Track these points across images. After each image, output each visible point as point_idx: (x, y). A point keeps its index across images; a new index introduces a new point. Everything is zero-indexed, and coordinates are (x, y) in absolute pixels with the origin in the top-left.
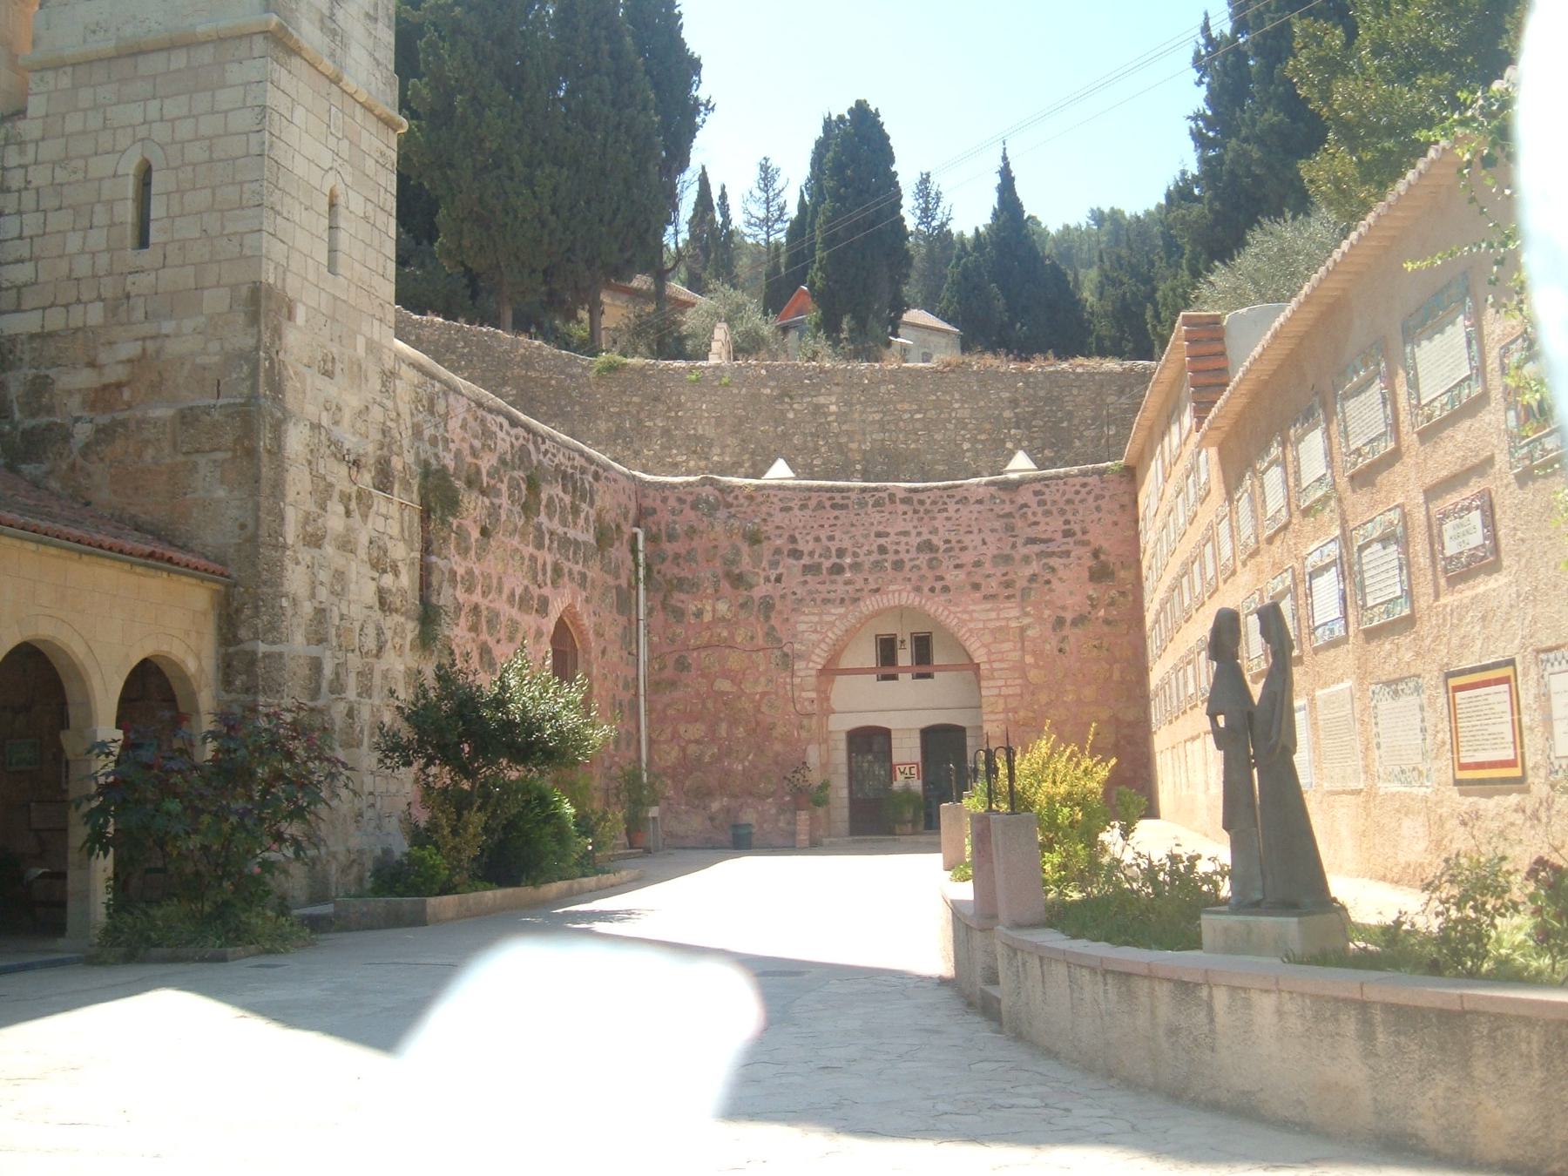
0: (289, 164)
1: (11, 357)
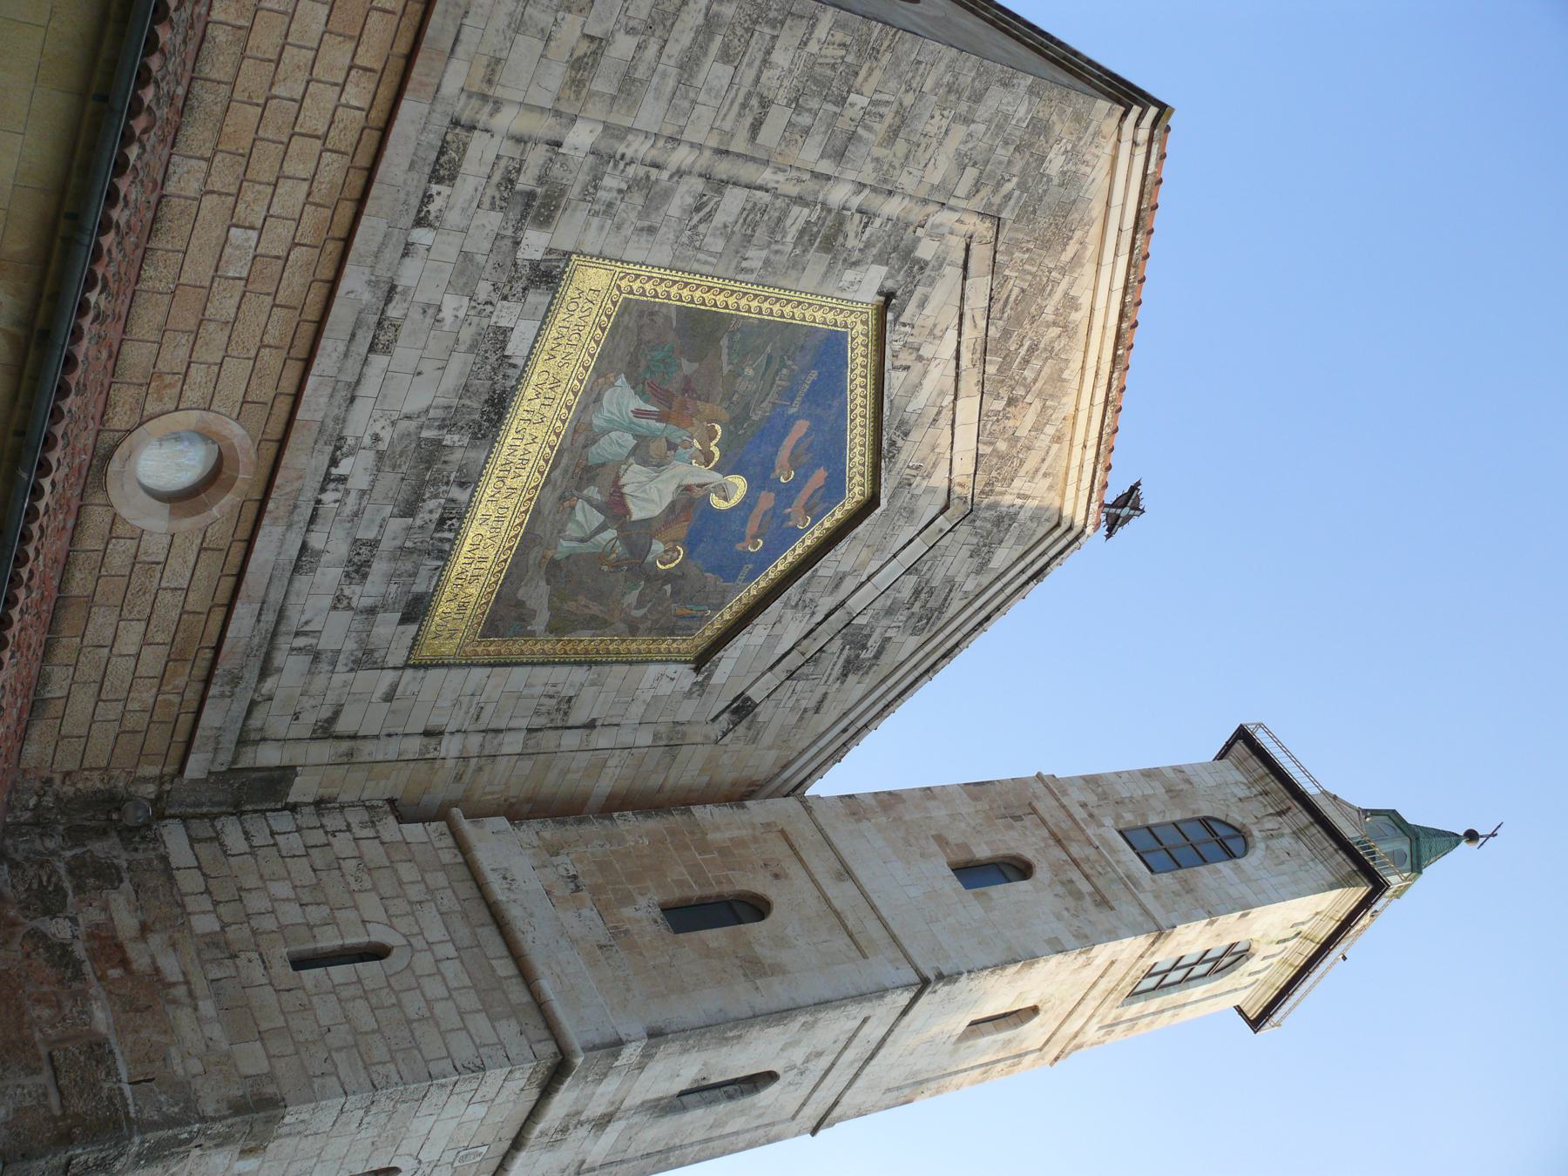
0: (424, 1110)
1: (137, 839)
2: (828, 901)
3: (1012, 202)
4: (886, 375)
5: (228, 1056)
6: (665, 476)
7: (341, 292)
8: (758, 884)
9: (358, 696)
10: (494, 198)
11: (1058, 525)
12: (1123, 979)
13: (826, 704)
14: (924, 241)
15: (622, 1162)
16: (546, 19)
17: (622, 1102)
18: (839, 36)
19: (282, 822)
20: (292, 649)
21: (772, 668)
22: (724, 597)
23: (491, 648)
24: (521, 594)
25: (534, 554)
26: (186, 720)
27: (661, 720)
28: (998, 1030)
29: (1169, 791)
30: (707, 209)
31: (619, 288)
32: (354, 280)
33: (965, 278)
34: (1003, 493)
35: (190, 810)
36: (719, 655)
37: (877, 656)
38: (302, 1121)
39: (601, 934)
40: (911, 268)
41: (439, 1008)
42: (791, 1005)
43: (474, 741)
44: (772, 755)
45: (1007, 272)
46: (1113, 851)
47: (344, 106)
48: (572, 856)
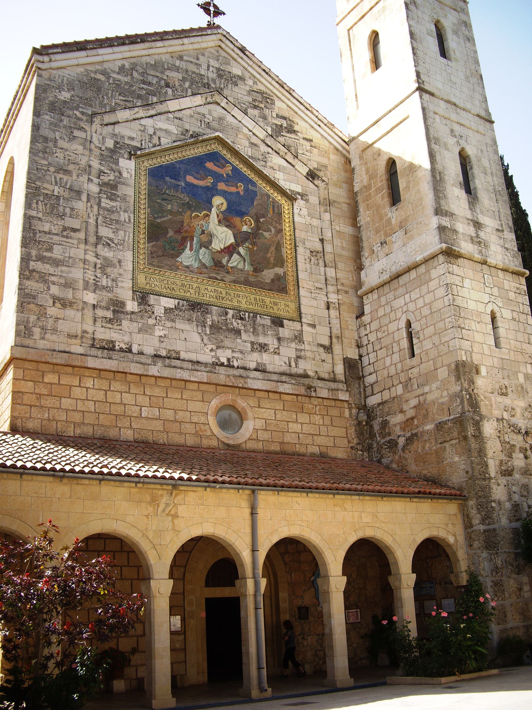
3: (84, 111)
5: (442, 381)
6: (215, 232)
7: (159, 375)
8: (382, 164)
9: (314, 339)
13: (308, 137)
14: (106, 146)
16: (51, 321)
17: (468, 219)
18: (34, 205)
19: (365, 360)
20: (296, 367)
21: (293, 166)
22: (264, 195)
23: (292, 288)
24: (268, 281)
25: (252, 279)
26: (326, 402)
30: (108, 241)
31: (143, 269)
32: (154, 370)
33: (119, 122)
34: (208, 78)
35: (362, 395)
36: (288, 191)
37: (285, 118)
38: (465, 353)
40: (118, 148)
41: (427, 301)
43: (331, 288)
44: (332, 157)
45: (113, 104)
47: (94, 386)
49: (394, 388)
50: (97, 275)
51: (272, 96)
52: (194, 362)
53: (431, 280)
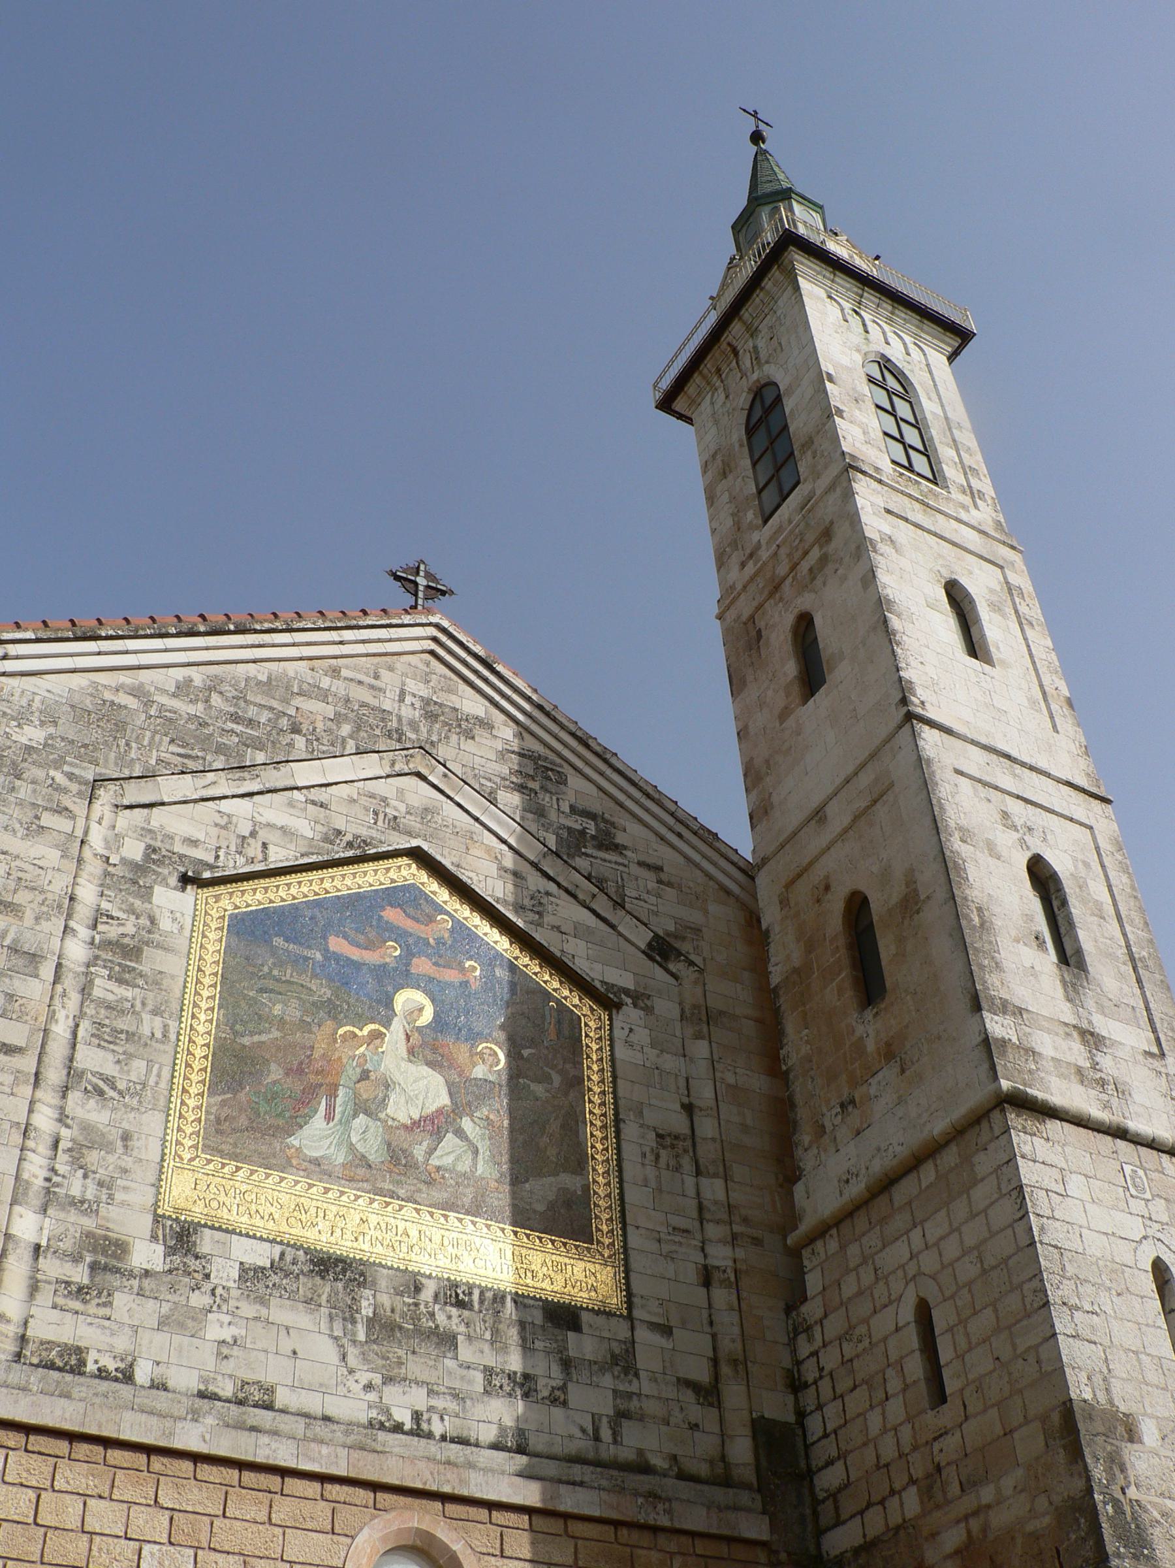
0: (1076, 1245)
2: (845, 831)
3: (76, 771)
4: (272, 866)
6: (398, 1077)
7: (204, 1449)
9: (668, 1364)
10: (98, 1305)
11: (432, 653)
12: (910, 496)
13: (650, 861)
14: (123, 855)
15: (1148, 1009)
17: (1066, 1024)
19: (814, 1425)
20: (615, 1442)
21: (613, 927)
23: (605, 1228)
26: (700, 1547)
27: (678, 1033)
28: (978, 620)
29: (724, 474)
30: (101, 1084)
32: (190, 1438)
33: (163, 804)
34: (400, 719)
35: (810, 1528)
36: (598, 984)
39: (889, 1073)
40: (154, 862)
41: (970, 1241)
42: (940, 859)
43: (712, 1231)
44: (713, 908)
45: (153, 762)
46: (780, 529)
48: (825, 1110)
49: (897, 1496)
50: (57, 1167)
51: (561, 766)
52: (315, 1418)
53: (975, 1182)
